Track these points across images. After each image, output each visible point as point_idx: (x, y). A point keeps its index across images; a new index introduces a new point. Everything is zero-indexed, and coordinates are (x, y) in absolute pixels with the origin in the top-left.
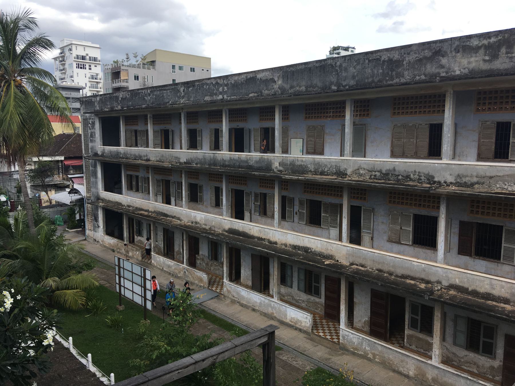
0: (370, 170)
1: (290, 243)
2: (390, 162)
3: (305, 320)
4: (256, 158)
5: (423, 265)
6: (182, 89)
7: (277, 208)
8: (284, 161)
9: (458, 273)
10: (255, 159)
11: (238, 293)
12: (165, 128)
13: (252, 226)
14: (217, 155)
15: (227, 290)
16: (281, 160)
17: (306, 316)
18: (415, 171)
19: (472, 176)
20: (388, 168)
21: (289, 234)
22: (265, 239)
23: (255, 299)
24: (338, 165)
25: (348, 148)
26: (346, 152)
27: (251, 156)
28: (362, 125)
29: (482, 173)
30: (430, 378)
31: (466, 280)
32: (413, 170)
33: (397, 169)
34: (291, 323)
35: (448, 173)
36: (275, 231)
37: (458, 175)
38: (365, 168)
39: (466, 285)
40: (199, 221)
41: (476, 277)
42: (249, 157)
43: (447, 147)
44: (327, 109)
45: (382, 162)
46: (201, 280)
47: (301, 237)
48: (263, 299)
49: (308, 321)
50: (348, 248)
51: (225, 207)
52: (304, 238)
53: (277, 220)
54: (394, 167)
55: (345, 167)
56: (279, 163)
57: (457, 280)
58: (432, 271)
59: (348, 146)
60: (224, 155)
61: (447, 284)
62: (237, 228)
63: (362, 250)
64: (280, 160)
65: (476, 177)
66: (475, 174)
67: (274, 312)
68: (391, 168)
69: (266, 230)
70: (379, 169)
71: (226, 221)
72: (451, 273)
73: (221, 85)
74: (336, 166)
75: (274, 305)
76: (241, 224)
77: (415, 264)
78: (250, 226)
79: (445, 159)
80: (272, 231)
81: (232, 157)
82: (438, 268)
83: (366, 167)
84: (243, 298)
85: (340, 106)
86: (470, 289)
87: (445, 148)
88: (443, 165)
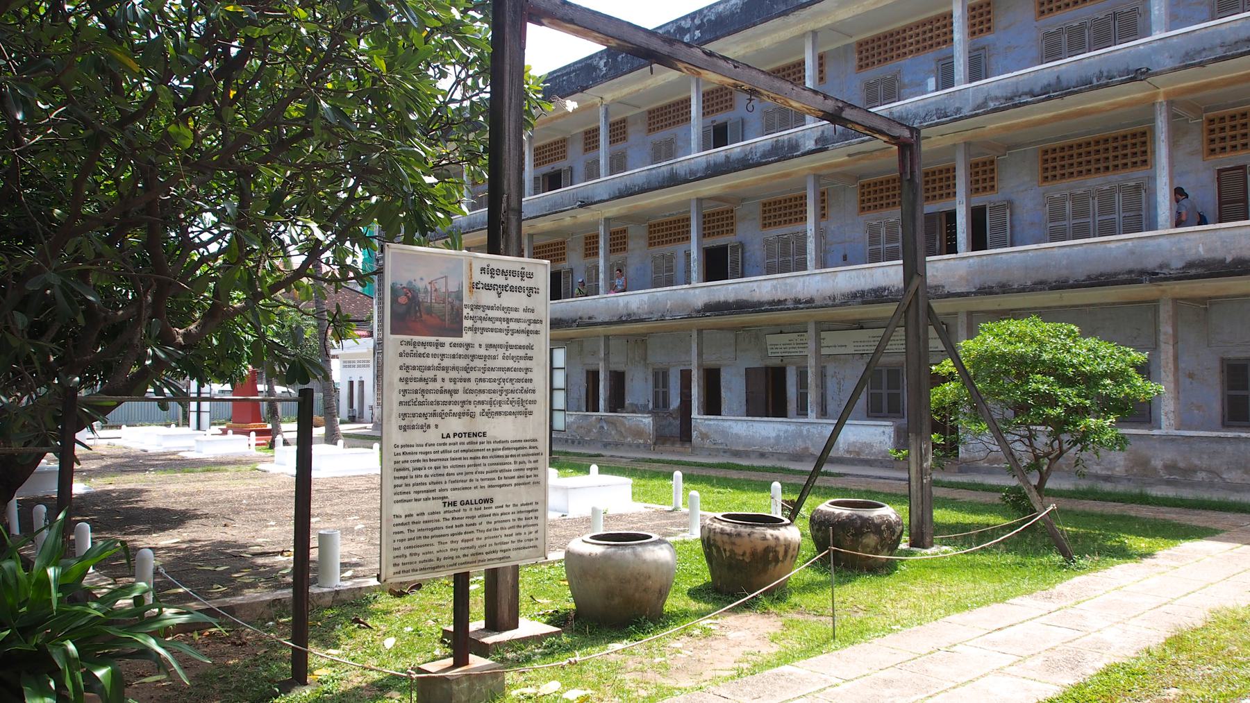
0: (1009, 95)
1: (843, 291)
2: (1049, 70)
3: (882, 438)
4: (764, 145)
5: (1130, 243)
6: (602, 63)
7: (813, 229)
8: (826, 133)
9: (1202, 235)
10: (761, 149)
11: (724, 433)
12: (553, 168)
13: (756, 284)
14: (678, 165)
15: (701, 433)
16: (820, 133)
17: (882, 429)
18: (1101, 72)
19: (1212, 48)
20: (1046, 82)
21: (840, 275)
22: (786, 300)
23: (764, 433)
24: (943, 107)
25: (962, 68)
26: (956, 78)
27: (753, 145)
28: (978, 50)
29: (1231, 38)
30: (1157, 463)
31: (1219, 243)
32: (1097, 71)
33: (1063, 78)
34: (848, 456)
35: (1166, 54)
36: (808, 278)
37: (1187, 54)
38: (999, 95)
39: (1219, 254)
40: (636, 310)
41: (1237, 232)
42: (749, 148)
43: (1159, 10)
44: (905, 39)
45: (1032, 74)
46: (638, 433)
47: (867, 272)
48: (784, 427)
49: (886, 438)
50: (971, 261)
51: (696, 263)
52: (874, 270)
53: (814, 253)
54: (1058, 78)
55: (957, 105)
56: (816, 141)
57: (1201, 249)
58: (1147, 248)
59: (960, 65)
60: (692, 161)
61: (1181, 265)
62: (722, 299)
63: (1000, 256)
64: (817, 134)
65: (1221, 46)
66: (1218, 41)
67: (809, 444)
68: (1053, 80)
69: (788, 281)
70: (1026, 90)
71: (697, 291)
72: (1187, 239)
73: (688, 30)
74: (938, 109)
75: (808, 431)
76: (730, 287)
77: (1113, 245)
78: (751, 284)
79: (1158, 32)
80: (801, 279)
81: (711, 159)
82: (1161, 240)
83: (998, 93)
84: (738, 436)
85: (930, 27)
86: (1229, 259)
87: (1157, 12)
88: (1154, 45)
